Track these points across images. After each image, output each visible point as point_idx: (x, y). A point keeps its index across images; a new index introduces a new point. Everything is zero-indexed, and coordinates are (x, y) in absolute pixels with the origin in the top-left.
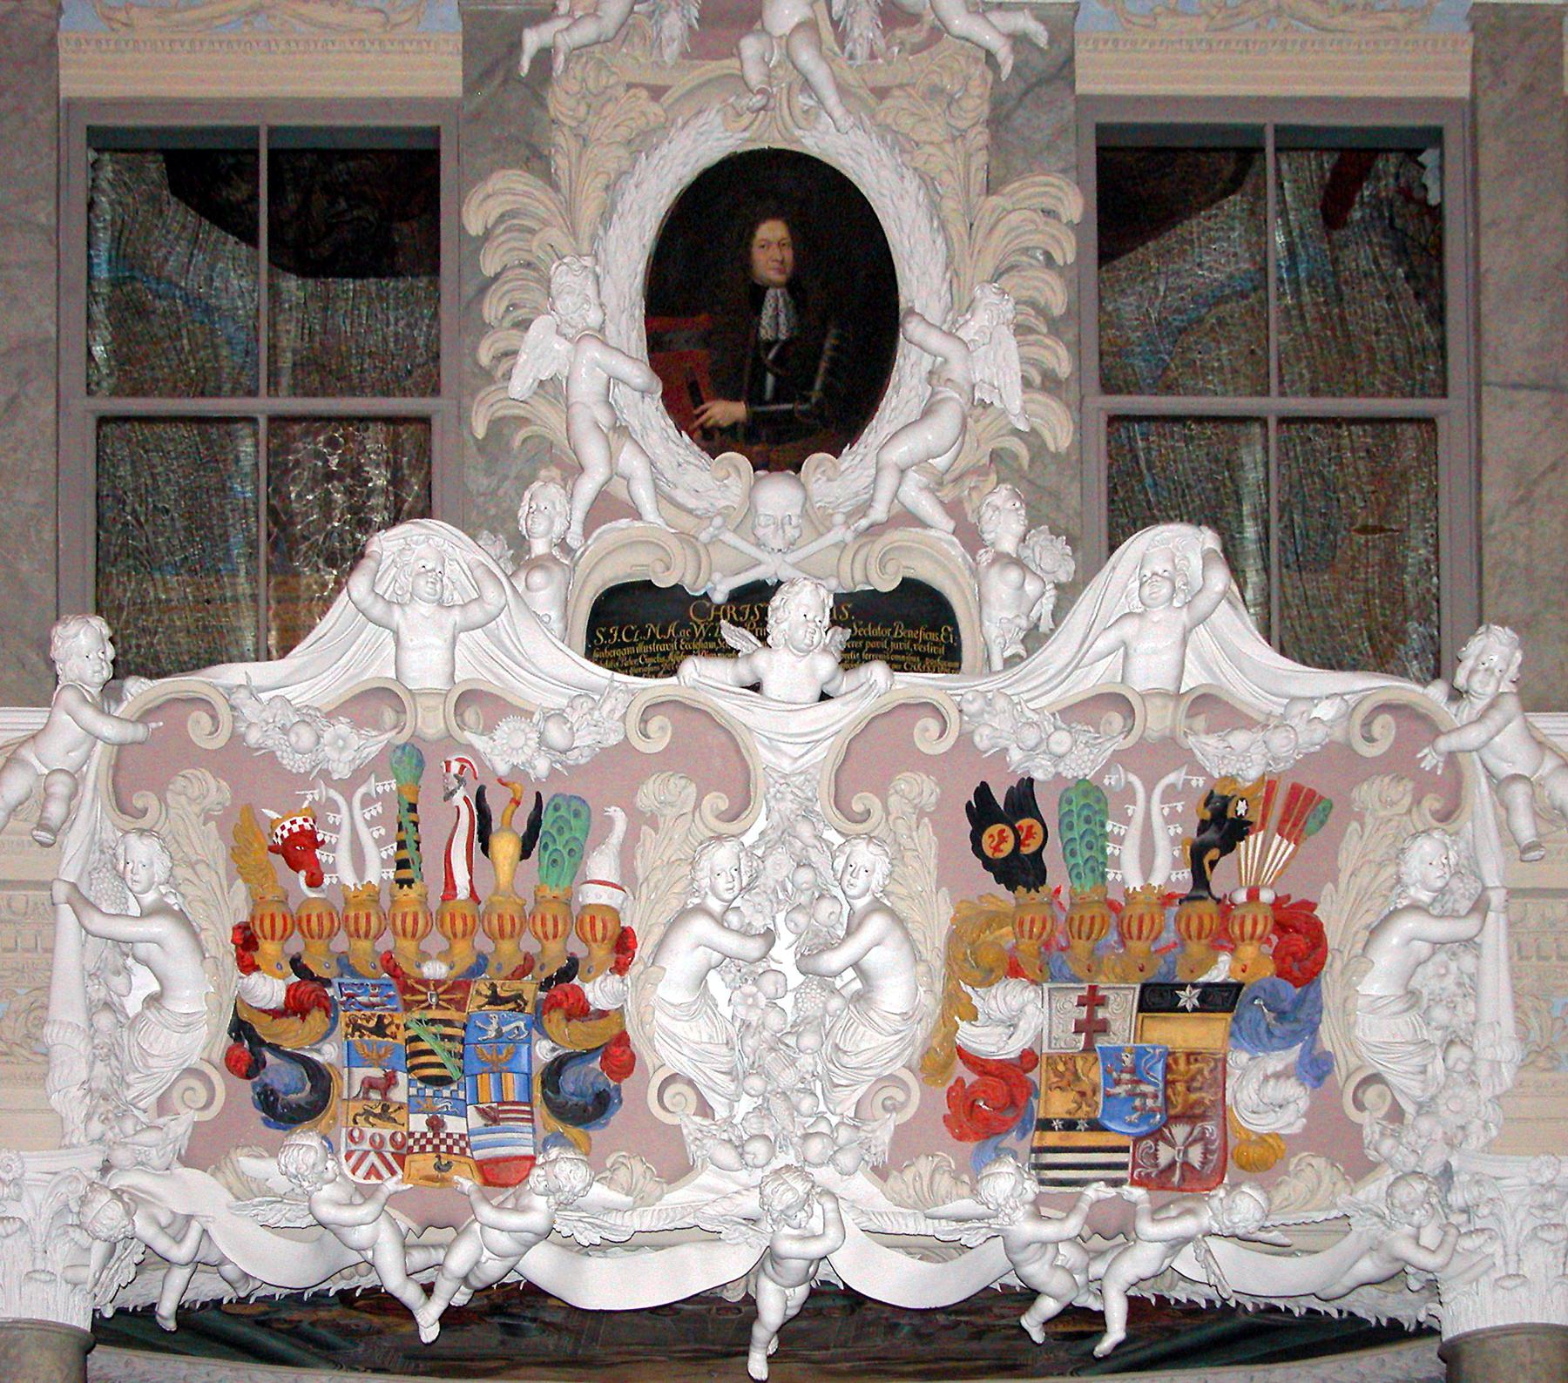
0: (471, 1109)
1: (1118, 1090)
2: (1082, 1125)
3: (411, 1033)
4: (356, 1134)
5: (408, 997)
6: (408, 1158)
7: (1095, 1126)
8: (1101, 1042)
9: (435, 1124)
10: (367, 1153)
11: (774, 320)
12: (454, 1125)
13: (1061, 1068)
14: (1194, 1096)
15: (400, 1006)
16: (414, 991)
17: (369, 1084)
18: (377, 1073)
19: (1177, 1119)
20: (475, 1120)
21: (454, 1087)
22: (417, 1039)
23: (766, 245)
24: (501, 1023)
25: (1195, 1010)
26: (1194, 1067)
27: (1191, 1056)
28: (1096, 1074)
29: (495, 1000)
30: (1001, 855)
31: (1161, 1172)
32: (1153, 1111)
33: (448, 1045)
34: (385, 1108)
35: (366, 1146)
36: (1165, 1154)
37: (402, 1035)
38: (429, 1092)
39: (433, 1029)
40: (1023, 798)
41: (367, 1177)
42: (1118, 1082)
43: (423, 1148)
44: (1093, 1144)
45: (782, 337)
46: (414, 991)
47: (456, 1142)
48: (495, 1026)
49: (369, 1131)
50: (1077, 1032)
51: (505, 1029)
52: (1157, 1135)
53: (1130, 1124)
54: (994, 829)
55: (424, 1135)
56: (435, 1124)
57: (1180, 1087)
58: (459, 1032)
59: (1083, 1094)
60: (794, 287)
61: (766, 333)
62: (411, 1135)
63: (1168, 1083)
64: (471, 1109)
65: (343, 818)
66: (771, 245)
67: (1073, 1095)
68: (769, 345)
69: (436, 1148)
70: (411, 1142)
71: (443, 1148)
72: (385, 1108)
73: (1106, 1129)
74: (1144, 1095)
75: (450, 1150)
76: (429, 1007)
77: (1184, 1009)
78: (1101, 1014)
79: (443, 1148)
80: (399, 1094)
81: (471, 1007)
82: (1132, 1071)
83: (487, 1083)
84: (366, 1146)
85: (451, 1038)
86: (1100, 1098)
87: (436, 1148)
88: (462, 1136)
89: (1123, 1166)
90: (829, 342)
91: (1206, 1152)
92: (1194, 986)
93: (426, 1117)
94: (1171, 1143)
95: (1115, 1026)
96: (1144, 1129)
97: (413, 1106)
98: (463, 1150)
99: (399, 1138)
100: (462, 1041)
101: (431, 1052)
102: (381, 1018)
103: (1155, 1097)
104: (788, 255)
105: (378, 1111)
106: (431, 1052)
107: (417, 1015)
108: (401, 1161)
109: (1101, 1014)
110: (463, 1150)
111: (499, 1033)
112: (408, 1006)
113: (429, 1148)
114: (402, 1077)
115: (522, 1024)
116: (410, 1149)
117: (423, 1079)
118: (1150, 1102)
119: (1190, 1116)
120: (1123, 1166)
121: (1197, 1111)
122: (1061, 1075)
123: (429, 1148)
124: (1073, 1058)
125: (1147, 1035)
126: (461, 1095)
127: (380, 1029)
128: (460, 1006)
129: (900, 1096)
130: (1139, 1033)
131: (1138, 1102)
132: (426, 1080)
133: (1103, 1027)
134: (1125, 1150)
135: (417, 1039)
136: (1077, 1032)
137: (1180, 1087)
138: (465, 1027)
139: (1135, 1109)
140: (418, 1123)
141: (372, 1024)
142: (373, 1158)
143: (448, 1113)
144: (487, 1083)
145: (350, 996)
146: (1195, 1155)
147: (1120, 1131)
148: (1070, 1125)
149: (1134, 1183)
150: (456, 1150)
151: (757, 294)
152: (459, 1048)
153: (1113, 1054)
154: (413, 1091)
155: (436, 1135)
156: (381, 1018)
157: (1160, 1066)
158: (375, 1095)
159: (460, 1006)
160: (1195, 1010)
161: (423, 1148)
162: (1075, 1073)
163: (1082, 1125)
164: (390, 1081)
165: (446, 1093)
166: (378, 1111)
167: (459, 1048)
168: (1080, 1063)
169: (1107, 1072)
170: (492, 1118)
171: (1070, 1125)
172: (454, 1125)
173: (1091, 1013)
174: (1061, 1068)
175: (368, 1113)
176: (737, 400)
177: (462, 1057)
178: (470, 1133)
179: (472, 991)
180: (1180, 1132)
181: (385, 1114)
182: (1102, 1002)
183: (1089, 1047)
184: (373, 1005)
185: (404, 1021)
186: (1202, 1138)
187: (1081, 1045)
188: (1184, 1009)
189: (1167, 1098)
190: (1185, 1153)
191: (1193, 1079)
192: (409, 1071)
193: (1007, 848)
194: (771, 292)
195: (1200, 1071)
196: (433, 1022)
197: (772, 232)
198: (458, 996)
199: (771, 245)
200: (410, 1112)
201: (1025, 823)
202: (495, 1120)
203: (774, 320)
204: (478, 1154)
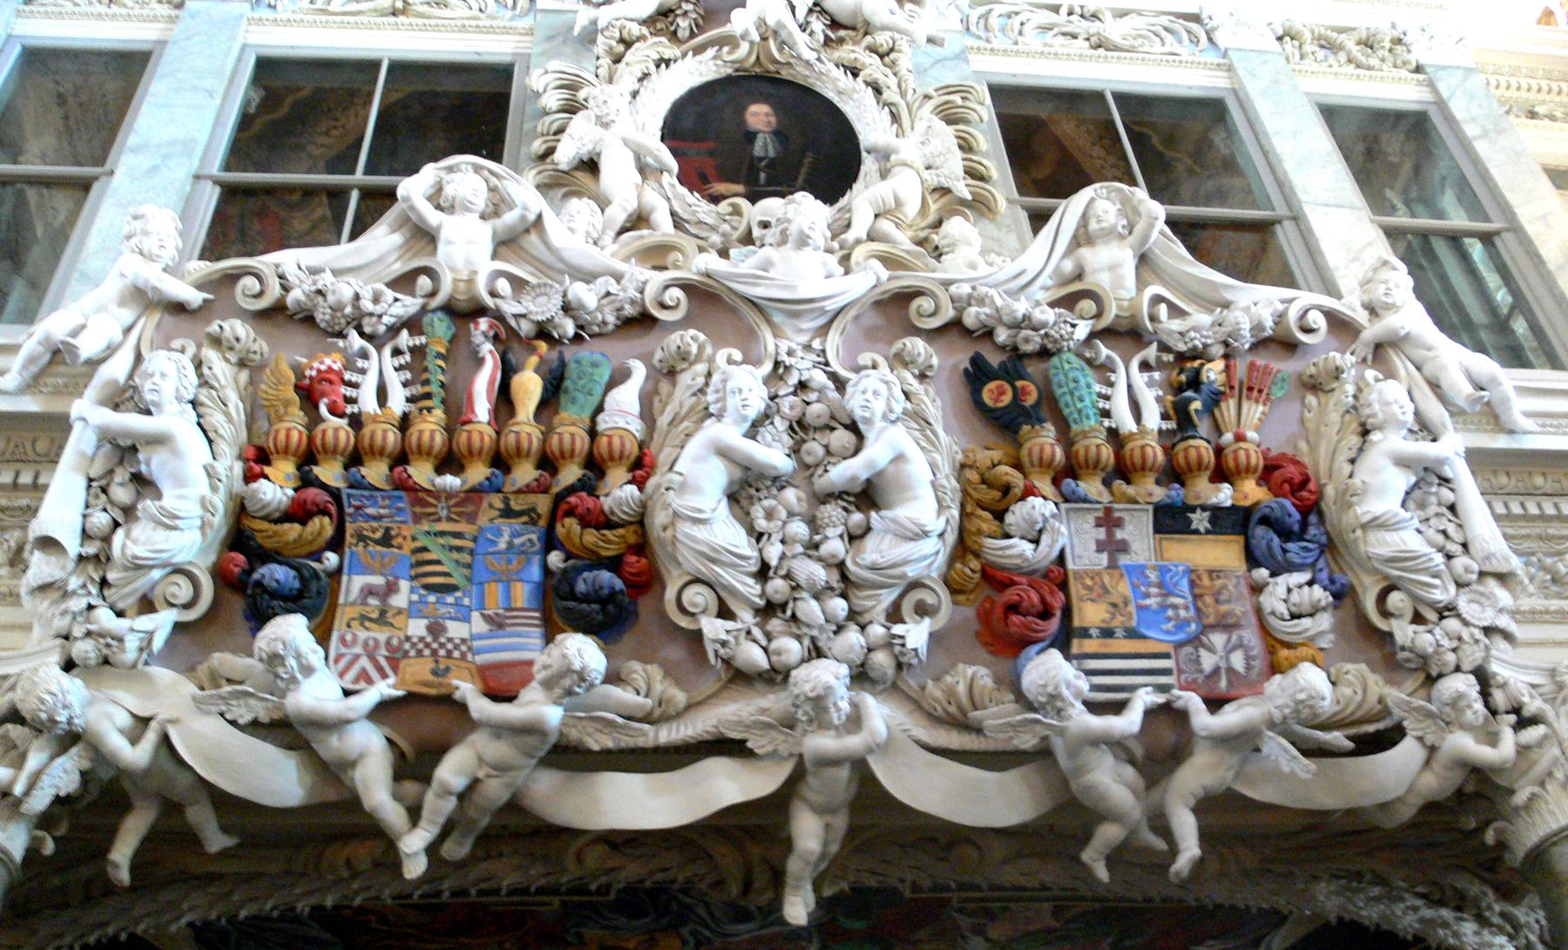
0: (475, 615)
1: (1148, 602)
2: (1119, 633)
3: (418, 544)
4: (349, 637)
5: (418, 510)
6: (402, 664)
7: (1132, 634)
8: (1124, 560)
9: (436, 629)
10: (357, 657)
12: (456, 630)
13: (1089, 582)
14: (1224, 608)
15: (410, 518)
16: (426, 504)
17: (369, 591)
18: (378, 580)
20: (478, 624)
21: (458, 594)
22: (424, 549)
23: (756, 114)
24: (514, 535)
25: (1208, 532)
26: (1218, 583)
27: (1211, 572)
28: (1124, 588)
29: (508, 513)
30: (1000, 405)
31: (1208, 677)
32: (1187, 622)
33: (455, 555)
34: (383, 613)
35: (358, 650)
36: (1208, 661)
37: (409, 546)
38: (432, 598)
39: (441, 541)
40: (1016, 362)
41: (356, 681)
42: (1147, 595)
43: (420, 653)
44: (1133, 651)
45: (772, 154)
46: (426, 504)
47: (456, 647)
48: (506, 537)
49: (362, 635)
50: (1099, 550)
51: (517, 541)
52: (1196, 641)
53: (1167, 632)
54: (992, 385)
55: (422, 639)
56: (436, 629)
57: (1209, 600)
58: (470, 544)
59: (1114, 605)
60: (777, 133)
61: (758, 149)
62: (408, 639)
63: (1196, 597)
64: (475, 615)
65: (372, 365)
66: (759, 115)
67: (1104, 607)
68: (761, 159)
69: (434, 653)
70: (407, 646)
71: (442, 652)
72: (383, 613)
73: (1144, 637)
74: (1175, 607)
75: (449, 654)
76: (439, 520)
77: (1196, 532)
78: (1119, 534)
79: (442, 652)
80: (400, 600)
81: (483, 521)
82: (1161, 585)
83: (495, 593)
84: (358, 650)
85: (459, 549)
86: (1132, 608)
87: (434, 653)
88: (464, 641)
89: (1166, 672)
90: (807, 160)
91: (1248, 658)
92: (1204, 508)
93: (424, 622)
94: (1211, 650)
95: (1134, 546)
96: (1180, 636)
97: (412, 611)
98: (463, 655)
99: (395, 642)
100: (472, 553)
101: (438, 562)
102: (388, 530)
103: (1187, 608)
104: (773, 120)
105: (375, 615)
106: (438, 562)
107: (426, 527)
108: (394, 663)
109: (1119, 534)
110: (463, 655)
111: (510, 545)
112: (417, 519)
113: (427, 652)
114: (404, 585)
115: (534, 537)
116: (406, 654)
117: (428, 587)
118: (1182, 613)
119: (1226, 625)
120: (1166, 672)
121: (1231, 621)
122: (1089, 588)
123: (427, 652)
124: (1098, 573)
125: (1166, 555)
126: (466, 601)
127: (386, 540)
128: (471, 518)
129: (931, 600)
130: (1159, 552)
131: (1170, 613)
132: (428, 587)
133: (1123, 547)
134: (1166, 656)
135: (424, 549)
136: (1099, 550)
137: (1209, 600)
138: (475, 540)
139: (1169, 619)
140: (417, 628)
141: (378, 535)
142: (364, 662)
143: (451, 618)
144: (495, 593)
145: (358, 508)
146: (1238, 660)
147: (1160, 637)
148: (1107, 633)
149: (1182, 688)
150: (456, 654)
151: (751, 136)
152: (466, 558)
153: (1141, 570)
154: (415, 597)
155: (435, 639)
156: (388, 530)
157: (1185, 582)
158: (373, 601)
159: (471, 518)
160: (1208, 532)
161: (420, 653)
162: (1104, 587)
163: (1119, 633)
164: (391, 588)
165: (450, 599)
166: (375, 615)
167: (466, 558)
168: (1106, 579)
169: (1134, 587)
170: (497, 624)
171: (1107, 633)
172: (456, 630)
173: (1110, 534)
174: (1089, 582)
175: (363, 618)
176: (738, 183)
177: (469, 566)
178: (473, 637)
179: (485, 505)
180: (1218, 639)
181: (382, 619)
182: (1119, 523)
183: (1113, 565)
184: (379, 518)
185: (411, 533)
186: (1240, 645)
187: (1105, 562)
188: (1196, 532)
189: (1198, 610)
190: (1227, 659)
191: (1219, 592)
192: (412, 578)
193: (1007, 399)
194: (760, 136)
195: (1225, 587)
196: (442, 534)
198: (469, 508)
199: (759, 115)
200: (410, 616)
201: (1019, 384)
202: (501, 626)
204: (479, 659)
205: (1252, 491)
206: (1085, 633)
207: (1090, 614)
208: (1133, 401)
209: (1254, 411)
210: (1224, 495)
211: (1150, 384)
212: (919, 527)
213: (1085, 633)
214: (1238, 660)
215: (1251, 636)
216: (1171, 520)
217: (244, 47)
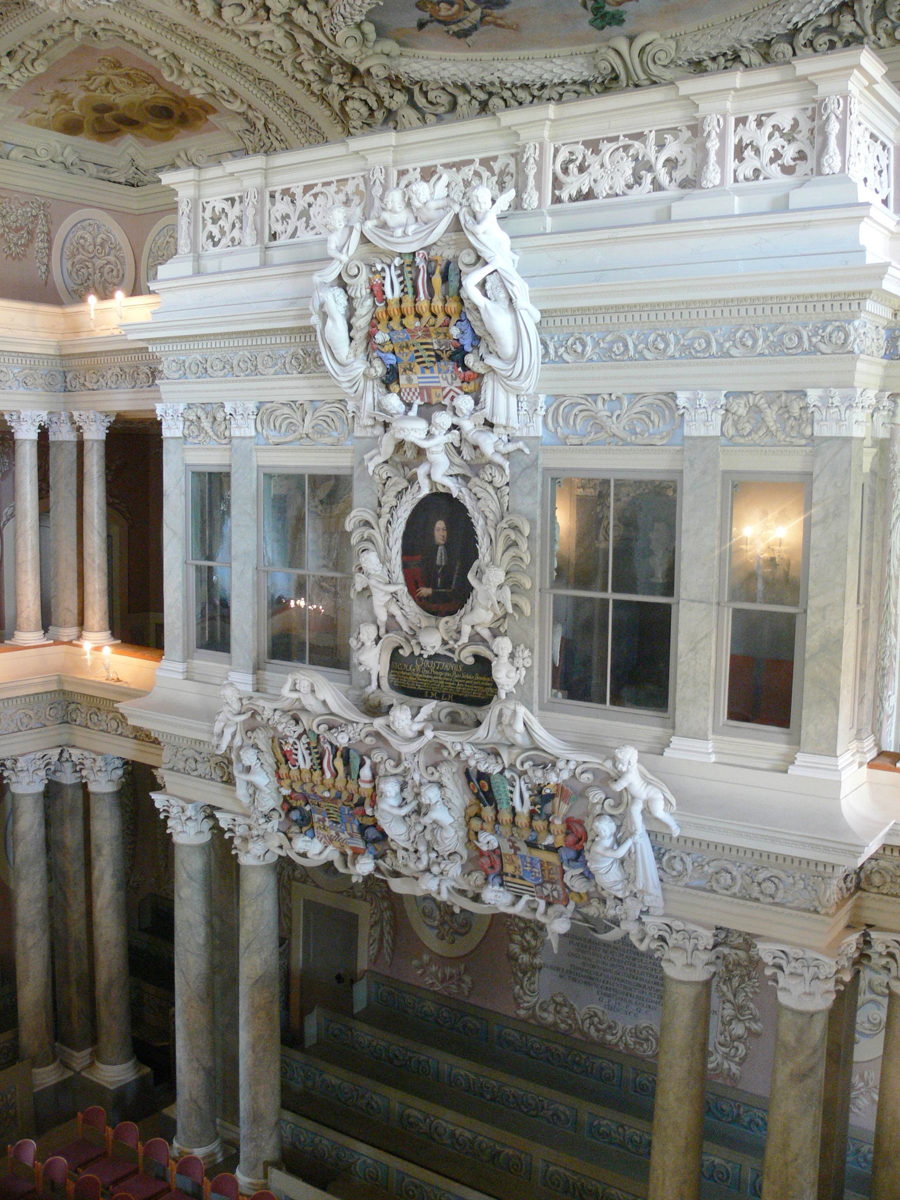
7: (521, 878)
11: (440, 558)
19: (548, 882)
28: (519, 862)
36: (546, 892)
60: (447, 545)
68: (439, 567)
104: (445, 533)
180: (549, 886)
183: (515, 853)
197: (440, 525)
203: (440, 558)
205: (560, 841)
206: (507, 875)
207: (509, 869)
208: (520, 800)
209: (564, 808)
210: (549, 840)
211: (528, 789)
212: (452, 838)
213: (507, 875)
214: (555, 894)
215: (559, 887)
216: (532, 845)
217: (258, 467)
